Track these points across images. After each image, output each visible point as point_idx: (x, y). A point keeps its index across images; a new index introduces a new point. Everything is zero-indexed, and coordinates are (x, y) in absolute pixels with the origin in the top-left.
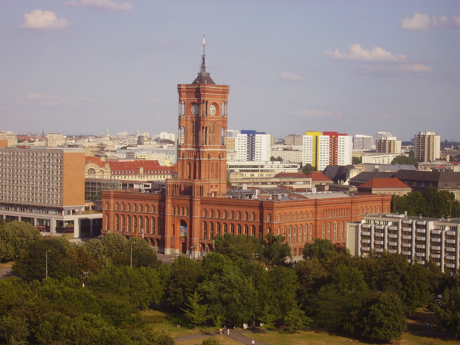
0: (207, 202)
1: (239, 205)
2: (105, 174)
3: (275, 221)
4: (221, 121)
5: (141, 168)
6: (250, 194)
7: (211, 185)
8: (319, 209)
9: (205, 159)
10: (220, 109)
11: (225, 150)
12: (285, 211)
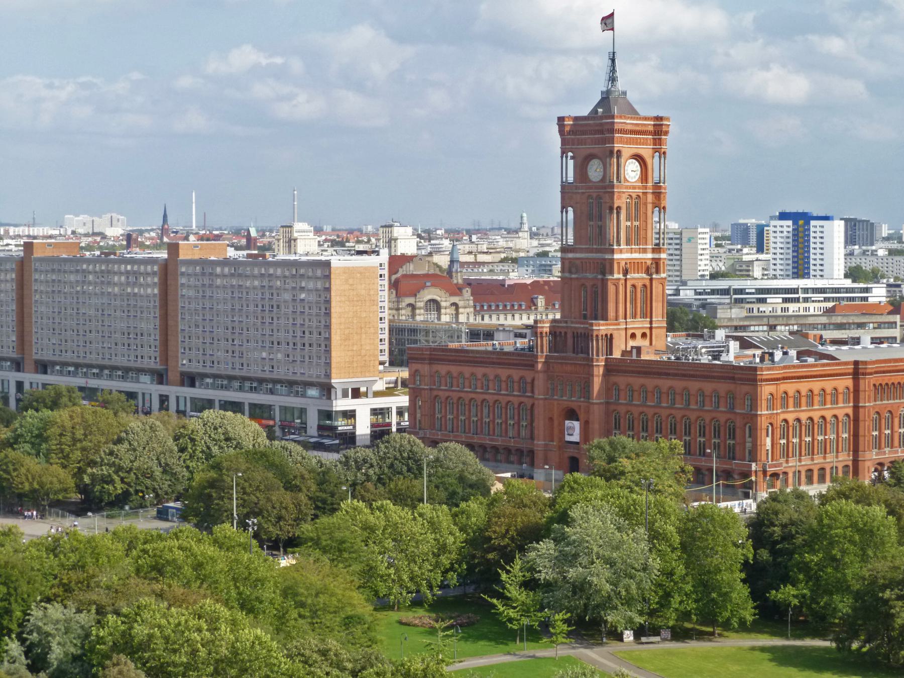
1: (684, 375)
3: (759, 408)
5: (541, 297)
6: (714, 351)
7: (630, 332)
9: (616, 276)
12: (783, 387)
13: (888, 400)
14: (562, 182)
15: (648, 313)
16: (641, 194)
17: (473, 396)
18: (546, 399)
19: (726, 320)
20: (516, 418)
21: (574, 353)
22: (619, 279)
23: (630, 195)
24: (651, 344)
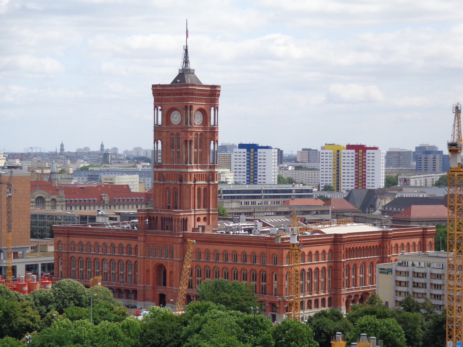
1: (234, 243)
2: (58, 203)
4: (210, 132)
7: (197, 217)
9: (189, 183)
10: (208, 116)
14: (155, 125)
15: (206, 206)
16: (203, 133)
17: (96, 256)
18: (144, 258)
19: (229, 210)
20: (125, 270)
21: (162, 229)
22: (191, 184)
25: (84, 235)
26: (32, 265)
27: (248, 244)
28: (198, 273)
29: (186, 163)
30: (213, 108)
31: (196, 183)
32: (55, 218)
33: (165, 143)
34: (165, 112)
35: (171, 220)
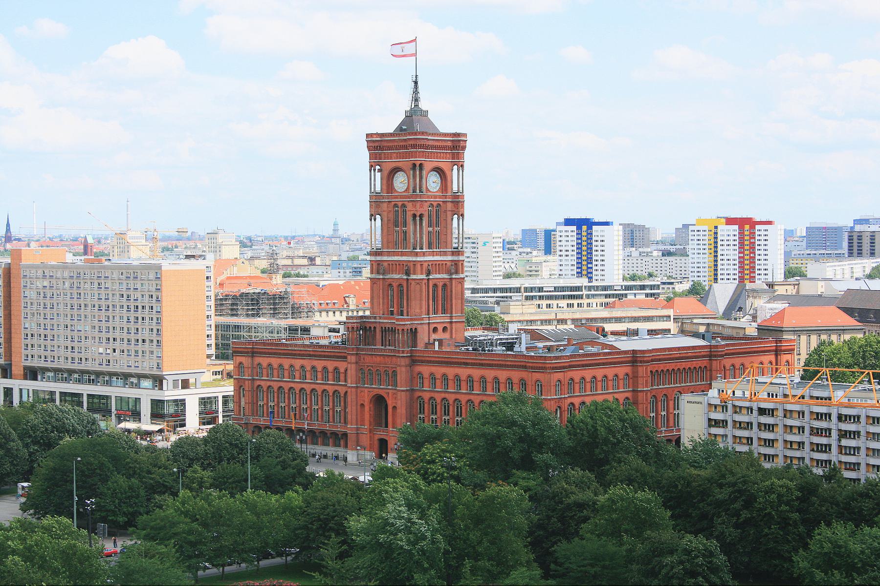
0: (423, 359)
1: (482, 365)
8: (642, 371)
11: (461, 258)
12: (570, 374)
13: (663, 385)
14: (371, 192)
16: (441, 203)
18: (357, 387)
20: (331, 404)
23: (431, 204)
24: (451, 337)
25: (275, 354)
26: (209, 398)
27: (501, 366)
28: (433, 409)
29: (415, 248)
30: (455, 167)
31: (431, 277)
32: (253, 329)
33: (385, 219)
34: (386, 173)
35: (393, 331)
